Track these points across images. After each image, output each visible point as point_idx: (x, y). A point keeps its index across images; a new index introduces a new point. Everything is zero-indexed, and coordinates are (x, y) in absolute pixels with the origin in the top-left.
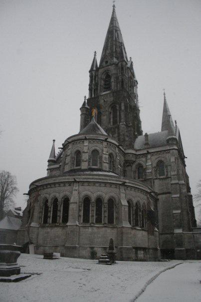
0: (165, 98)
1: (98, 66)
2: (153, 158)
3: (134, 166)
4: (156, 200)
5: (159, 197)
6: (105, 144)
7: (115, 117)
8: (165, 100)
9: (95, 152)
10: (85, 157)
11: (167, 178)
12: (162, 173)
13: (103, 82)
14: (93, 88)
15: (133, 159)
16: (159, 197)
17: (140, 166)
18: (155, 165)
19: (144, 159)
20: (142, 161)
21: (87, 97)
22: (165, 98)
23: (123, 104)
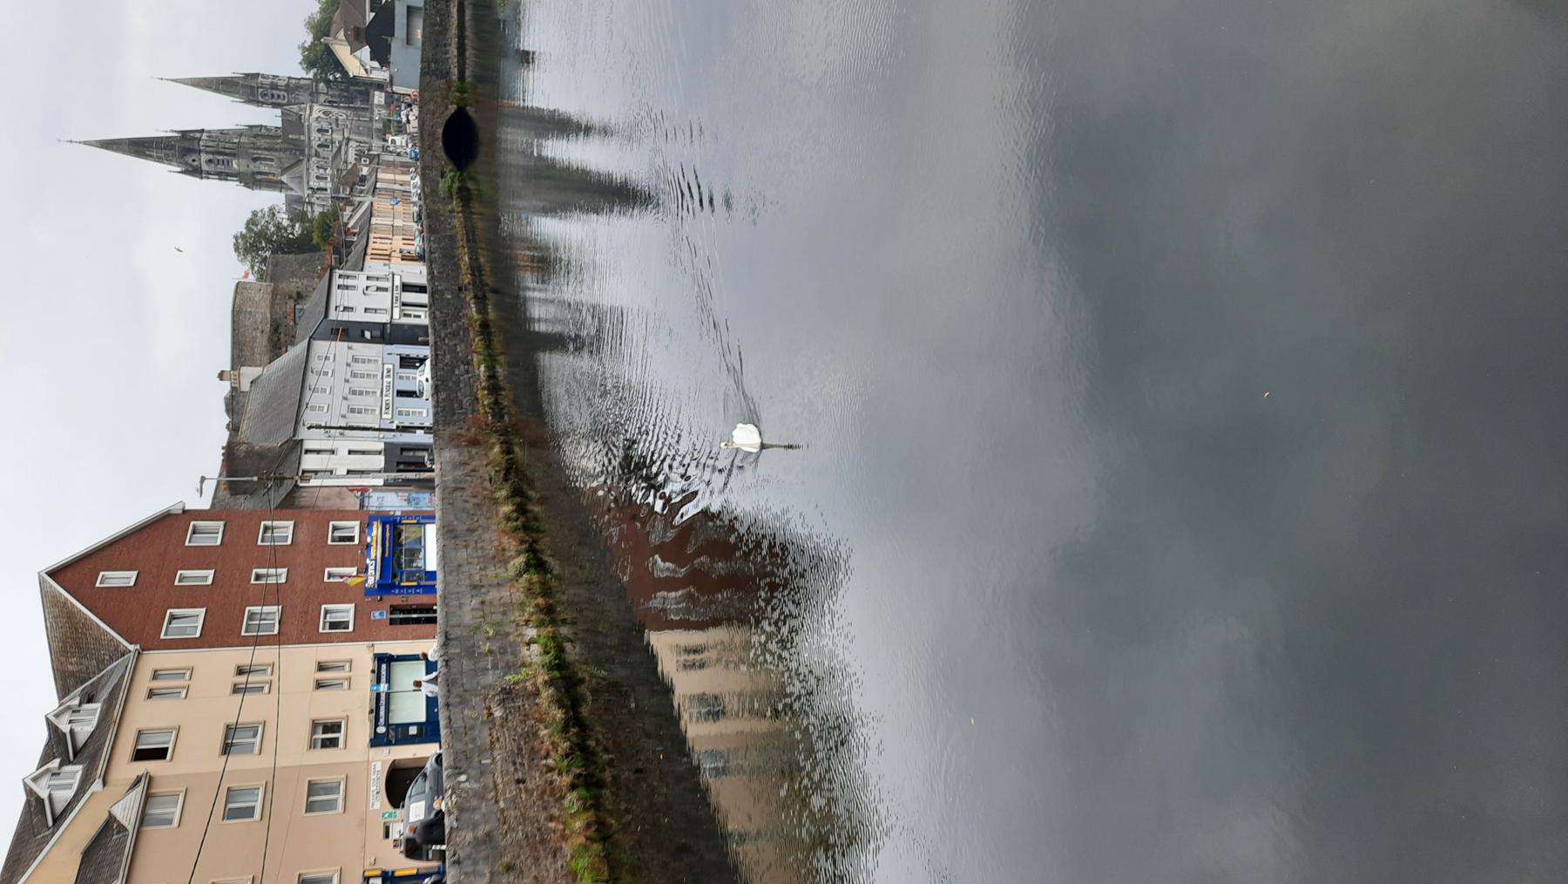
0: (168, 80)
1: (179, 169)
2: (314, 135)
3: (319, 150)
4: (349, 139)
5: (346, 136)
6: (310, 170)
7: (265, 159)
8: (173, 80)
9: (317, 177)
10: (322, 185)
11: (331, 128)
12: (327, 131)
13: (219, 166)
14: (223, 176)
15: (314, 151)
16: (346, 136)
17: (319, 146)
18: (320, 135)
19: (314, 142)
20: (315, 144)
21: (238, 183)
22: (168, 80)
23: (255, 151)
